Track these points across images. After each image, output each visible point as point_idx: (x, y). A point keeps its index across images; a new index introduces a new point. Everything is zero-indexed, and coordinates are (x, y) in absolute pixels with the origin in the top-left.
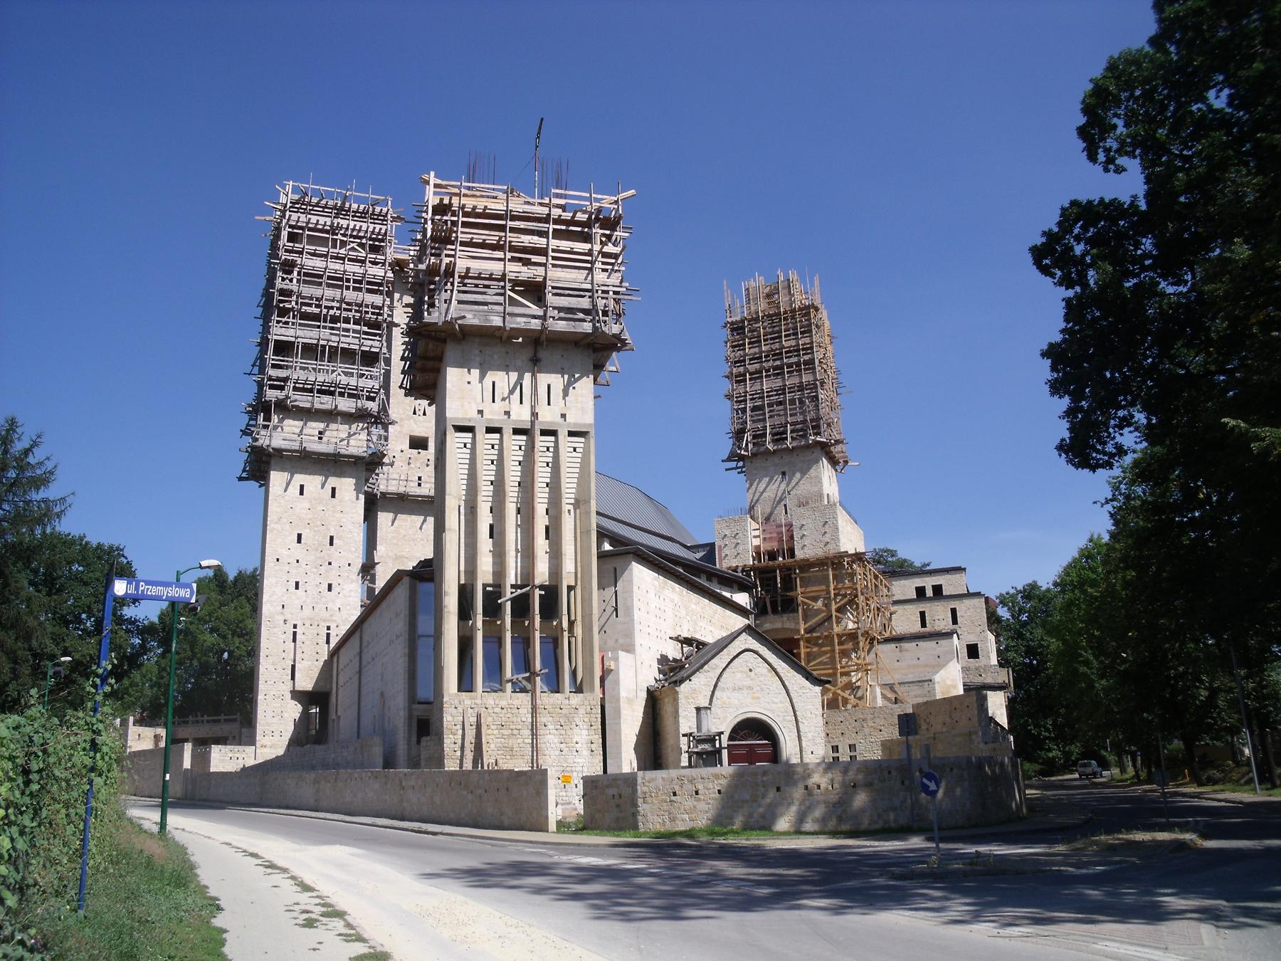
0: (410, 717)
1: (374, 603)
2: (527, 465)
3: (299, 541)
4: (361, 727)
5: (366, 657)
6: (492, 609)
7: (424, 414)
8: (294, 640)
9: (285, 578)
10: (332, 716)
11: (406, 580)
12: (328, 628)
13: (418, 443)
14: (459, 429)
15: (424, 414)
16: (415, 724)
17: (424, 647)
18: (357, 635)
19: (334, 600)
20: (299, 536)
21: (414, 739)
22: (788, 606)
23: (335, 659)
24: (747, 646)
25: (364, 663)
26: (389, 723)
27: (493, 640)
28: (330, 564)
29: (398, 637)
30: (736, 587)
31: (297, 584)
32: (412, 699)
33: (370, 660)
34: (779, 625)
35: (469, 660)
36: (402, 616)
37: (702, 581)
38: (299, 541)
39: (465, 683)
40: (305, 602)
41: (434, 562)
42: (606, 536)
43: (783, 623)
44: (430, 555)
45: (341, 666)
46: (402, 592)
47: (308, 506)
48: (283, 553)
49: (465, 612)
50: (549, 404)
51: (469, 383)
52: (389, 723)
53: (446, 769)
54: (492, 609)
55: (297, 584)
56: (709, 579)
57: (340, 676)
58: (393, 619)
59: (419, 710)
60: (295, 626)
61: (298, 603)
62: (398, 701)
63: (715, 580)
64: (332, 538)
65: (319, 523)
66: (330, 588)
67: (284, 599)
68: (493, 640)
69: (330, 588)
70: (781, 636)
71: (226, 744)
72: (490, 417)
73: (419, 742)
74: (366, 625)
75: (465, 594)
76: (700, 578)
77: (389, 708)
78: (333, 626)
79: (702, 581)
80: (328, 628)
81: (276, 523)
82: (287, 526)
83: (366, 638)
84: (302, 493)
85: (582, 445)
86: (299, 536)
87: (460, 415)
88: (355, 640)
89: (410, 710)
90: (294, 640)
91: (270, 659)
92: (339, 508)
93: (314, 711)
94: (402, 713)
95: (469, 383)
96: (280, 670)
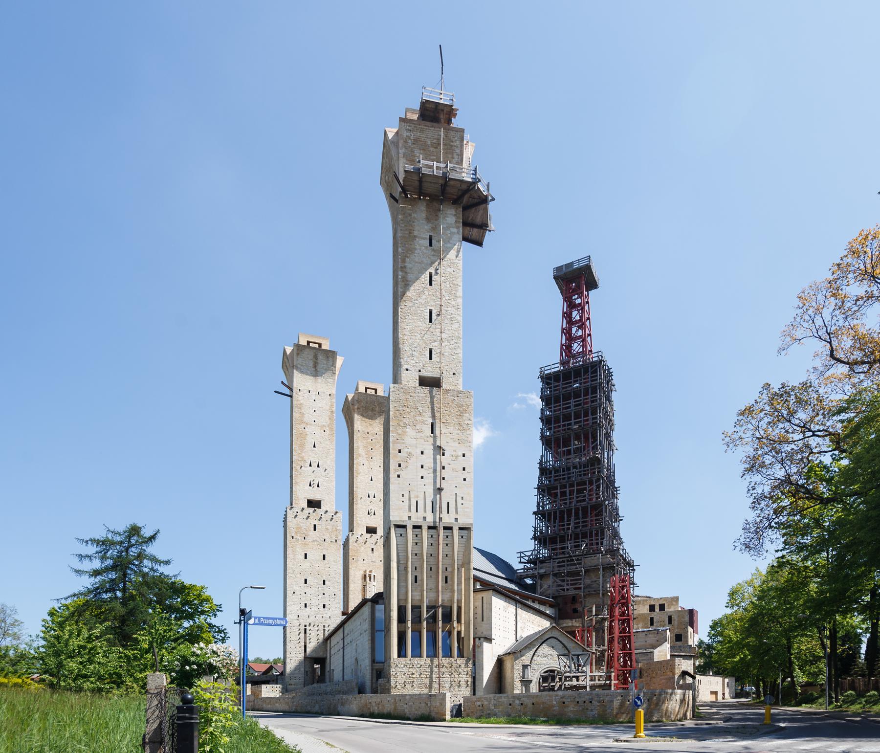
0: (372, 670)
1: (348, 616)
2: (432, 544)
3: (306, 582)
4: (345, 674)
5: (347, 641)
6: (417, 620)
7: (374, 514)
8: (305, 632)
9: (298, 601)
10: (328, 669)
11: (369, 603)
12: (324, 626)
13: (371, 531)
14: (398, 526)
15: (374, 514)
16: (375, 672)
17: (379, 636)
18: (341, 630)
19: (327, 613)
20: (306, 580)
21: (375, 680)
22: (576, 614)
23: (329, 642)
24: (555, 636)
25: (345, 644)
26: (360, 672)
27: (417, 633)
28: (324, 594)
29: (365, 631)
30: (548, 605)
31: (306, 605)
32: (373, 661)
33: (349, 642)
34: (570, 624)
35: (404, 646)
36: (367, 621)
37: (530, 603)
38: (306, 582)
39: (401, 653)
40: (310, 614)
41: (384, 594)
42: (478, 581)
43: (572, 623)
44: (381, 590)
45: (332, 645)
46: (366, 610)
47: (310, 564)
48: (297, 589)
49: (402, 619)
50: (448, 513)
51: (403, 501)
52: (360, 672)
53: (394, 692)
54: (417, 620)
55: (306, 605)
56: (533, 602)
57: (332, 650)
58: (361, 623)
59: (377, 666)
60: (305, 626)
61: (306, 615)
62: (366, 663)
63: (536, 602)
64: (324, 581)
65: (316, 573)
66: (324, 606)
67: (298, 612)
68: (417, 633)
69: (324, 606)
70: (569, 630)
71: (269, 684)
72: (414, 520)
73: (377, 680)
74: (346, 626)
75: (402, 610)
76: (528, 601)
77: (361, 665)
78: (327, 626)
79: (530, 603)
80: (324, 626)
81: (292, 574)
82: (298, 575)
83: (346, 632)
84: (306, 557)
85: (466, 535)
86: (306, 580)
87: (398, 519)
88: (340, 633)
89: (372, 666)
90: (305, 632)
91: (292, 643)
92: (328, 566)
93: (317, 666)
94: (368, 668)
95: (403, 501)
96: (298, 648)
